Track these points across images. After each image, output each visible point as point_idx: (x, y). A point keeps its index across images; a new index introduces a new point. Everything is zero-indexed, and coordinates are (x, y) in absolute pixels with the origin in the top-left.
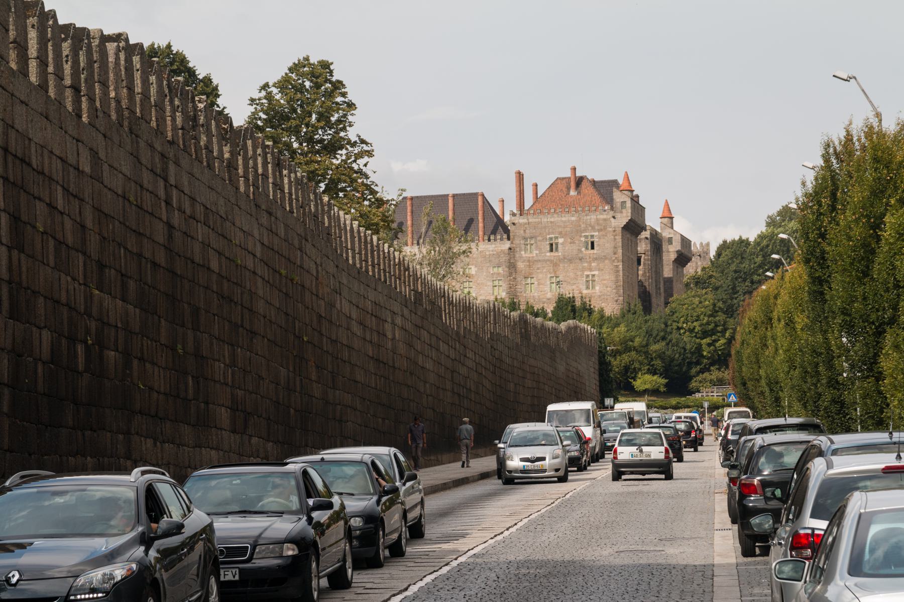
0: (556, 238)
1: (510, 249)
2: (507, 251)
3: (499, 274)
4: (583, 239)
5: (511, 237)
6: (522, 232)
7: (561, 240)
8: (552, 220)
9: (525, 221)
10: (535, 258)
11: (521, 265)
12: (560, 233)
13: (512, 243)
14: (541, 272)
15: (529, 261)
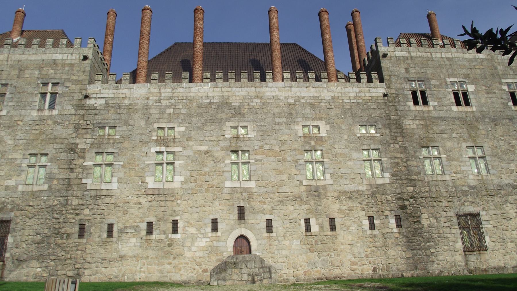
0: (461, 83)
1: (385, 95)
2: (381, 99)
3: (372, 137)
4: (505, 87)
5: (386, 77)
6: (403, 71)
7: (471, 88)
8: (449, 55)
9: (405, 54)
10: (434, 114)
11: (410, 124)
12: (467, 76)
13: (388, 87)
14: (450, 138)
15: (423, 118)
